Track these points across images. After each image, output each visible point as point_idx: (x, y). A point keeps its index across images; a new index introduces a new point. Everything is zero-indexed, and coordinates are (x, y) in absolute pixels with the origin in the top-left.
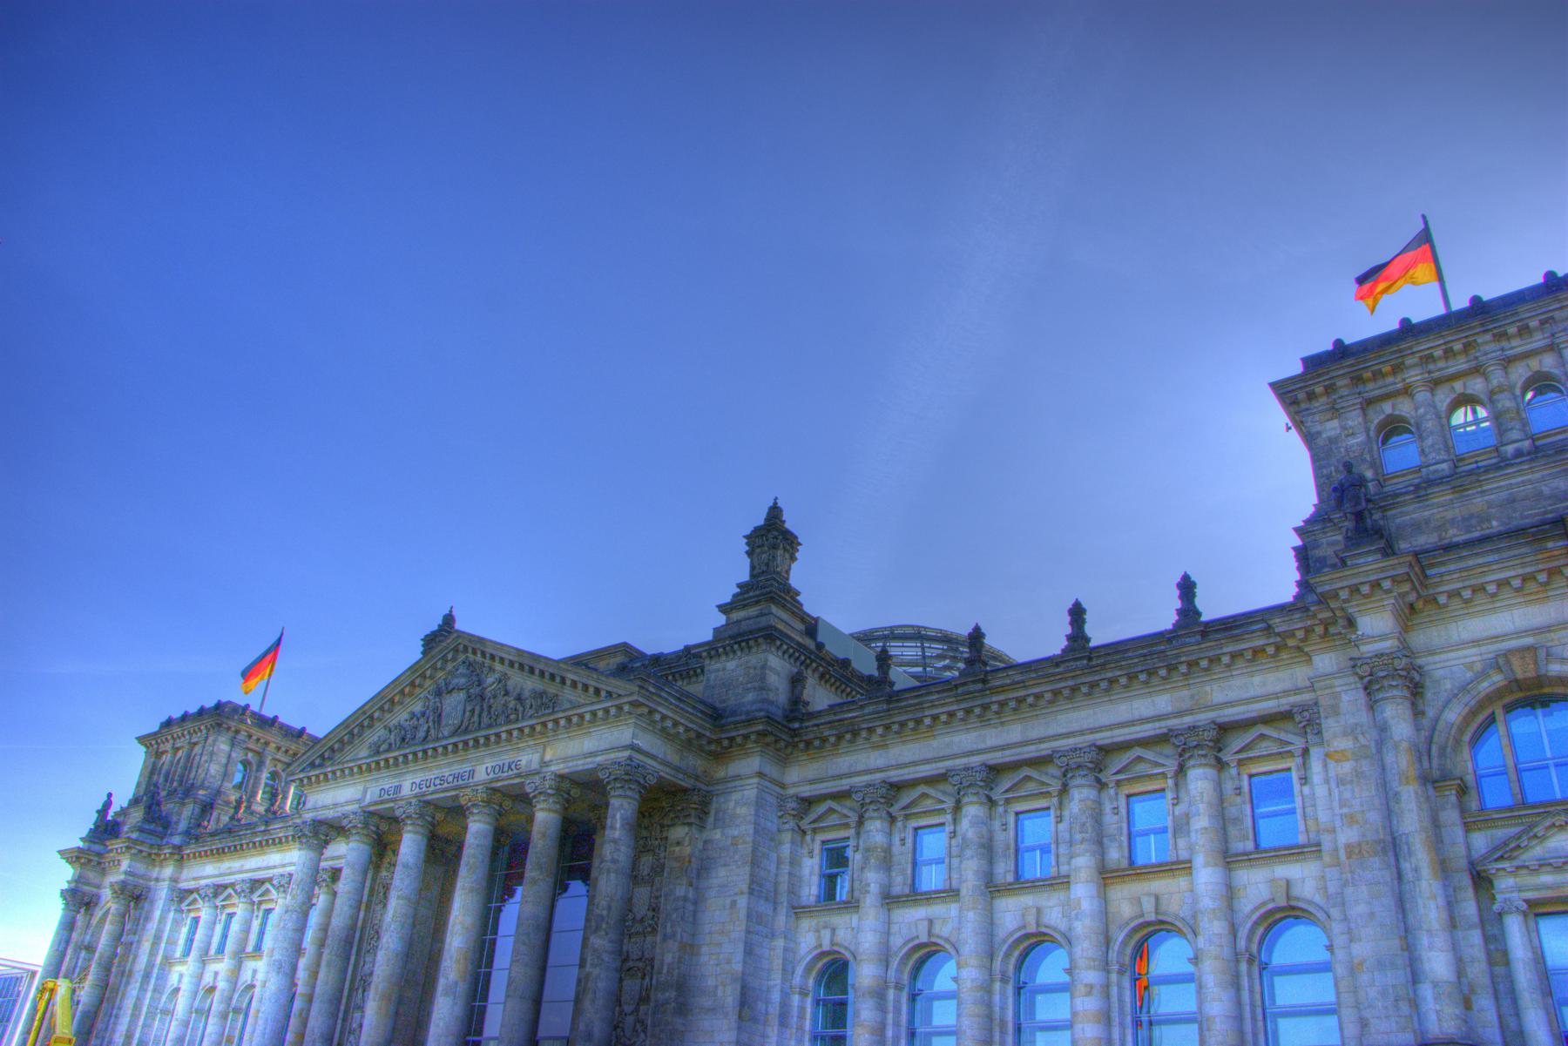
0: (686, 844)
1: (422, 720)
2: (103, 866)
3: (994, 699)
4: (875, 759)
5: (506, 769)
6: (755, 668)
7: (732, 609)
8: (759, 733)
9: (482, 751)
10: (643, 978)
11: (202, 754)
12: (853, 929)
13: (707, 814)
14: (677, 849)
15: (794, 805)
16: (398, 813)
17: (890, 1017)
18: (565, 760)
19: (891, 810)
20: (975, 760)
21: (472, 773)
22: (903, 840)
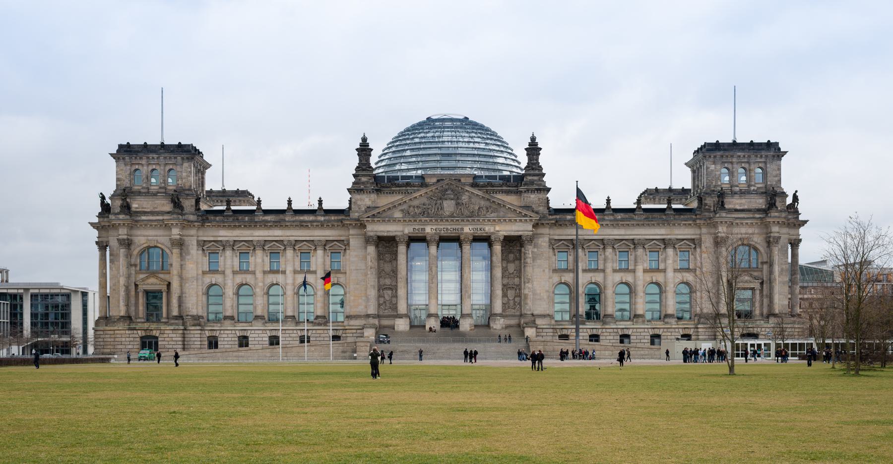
1: (430, 206)
3: (621, 223)
5: (479, 230)
8: (552, 223)
9: (467, 223)
10: (516, 290)
16: (428, 238)
18: (506, 231)
22: (585, 255)
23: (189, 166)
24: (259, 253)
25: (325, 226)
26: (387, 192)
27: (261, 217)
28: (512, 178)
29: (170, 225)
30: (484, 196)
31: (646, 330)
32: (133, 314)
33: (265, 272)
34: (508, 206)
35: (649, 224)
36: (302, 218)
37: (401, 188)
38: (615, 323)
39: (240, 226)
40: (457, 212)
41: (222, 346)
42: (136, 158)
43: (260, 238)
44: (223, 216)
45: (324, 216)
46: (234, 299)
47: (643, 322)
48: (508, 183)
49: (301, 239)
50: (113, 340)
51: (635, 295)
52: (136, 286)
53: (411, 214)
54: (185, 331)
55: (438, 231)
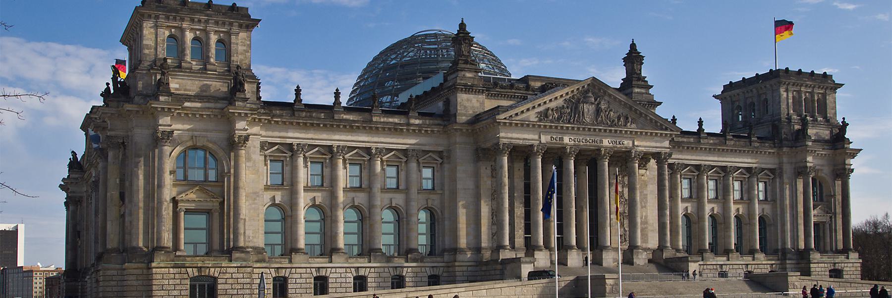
5: (618, 143)
11: (237, 44)
14: (643, 177)
18: (645, 147)
20: (707, 163)
21: (601, 142)
23: (248, 37)
26: (492, 94)
35: (740, 151)
36: (391, 120)
37: (506, 90)
39: (318, 125)
41: (294, 291)
42: (175, 19)
43: (342, 143)
45: (419, 119)
50: (140, 282)
51: (728, 228)
52: (174, 201)
55: (577, 142)
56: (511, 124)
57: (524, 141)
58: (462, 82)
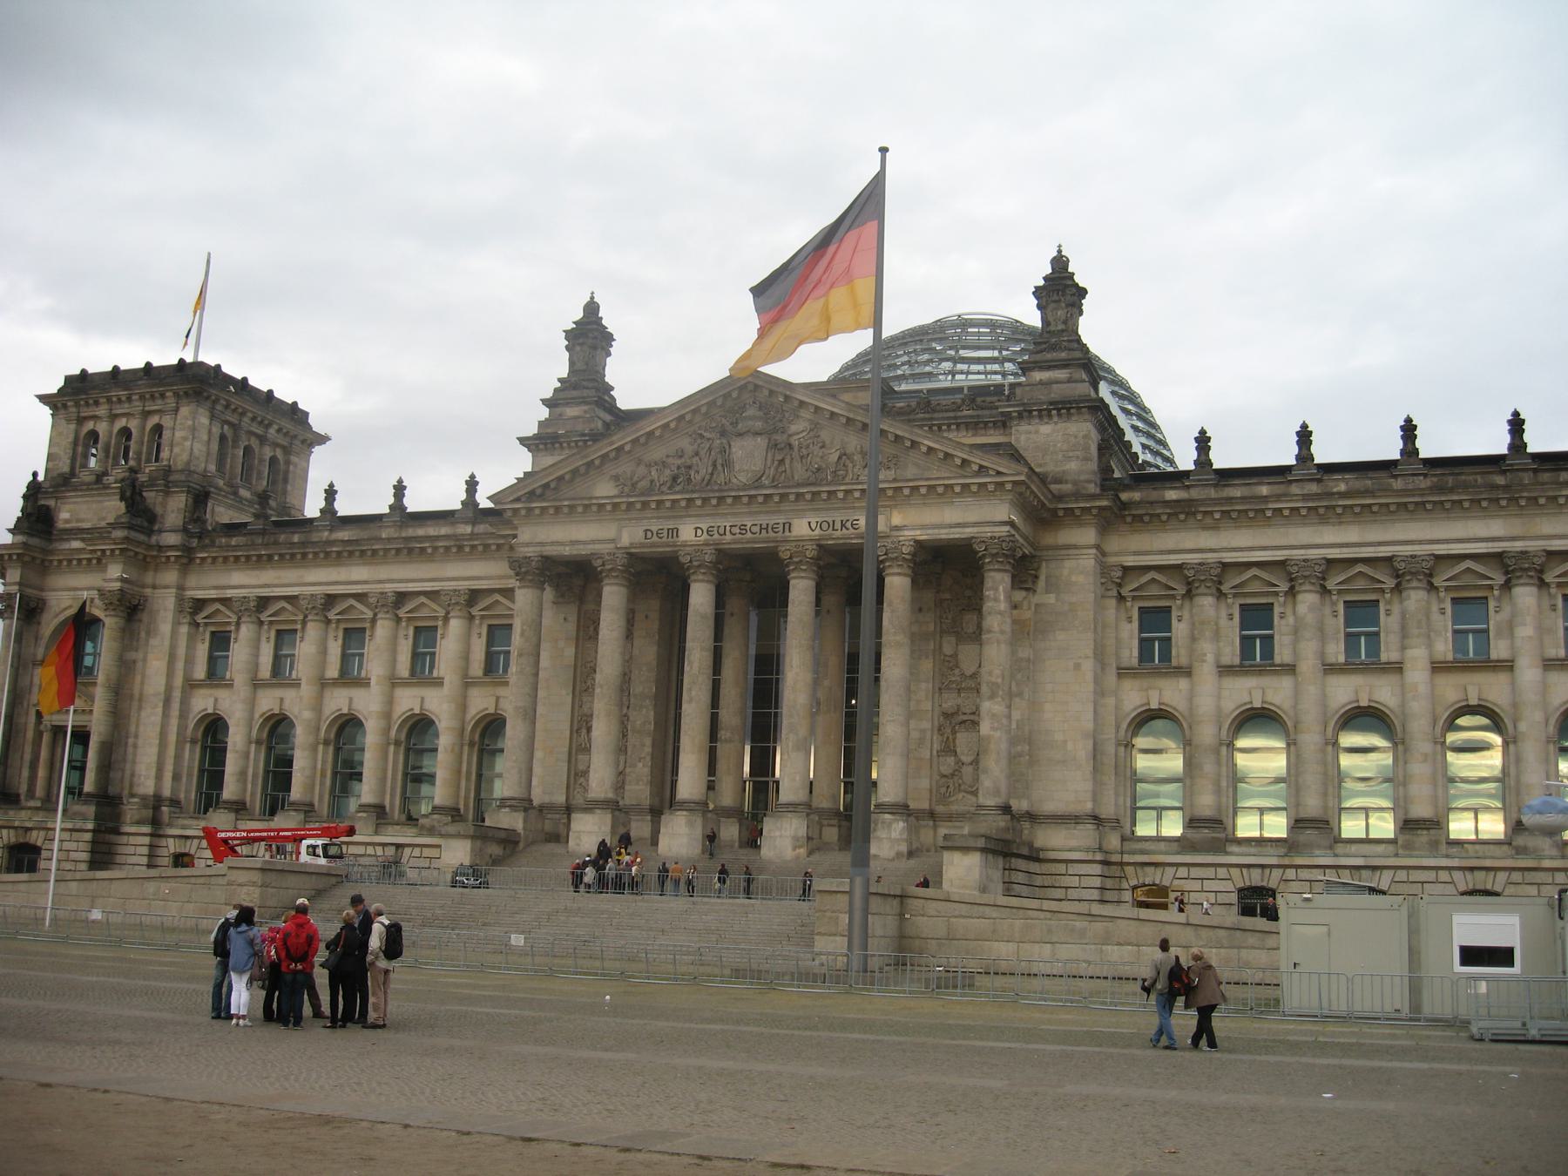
0: (1025, 608)
2: (47, 564)
3: (1340, 503)
4: (1206, 539)
5: (838, 525)
6: (1076, 437)
7: (1034, 368)
8: (1101, 508)
12: (1180, 691)
13: (1036, 577)
15: (1119, 574)
16: (685, 560)
17: (1224, 769)
18: (923, 527)
19: (1222, 588)
21: (788, 526)
22: (1230, 616)
24: (313, 630)
25: (467, 549)
27: (326, 534)
28: (1006, 393)
29: (99, 553)
30: (851, 416)
31: (1444, 875)
32: (23, 788)
33: (323, 684)
34: (926, 442)
35: (1442, 502)
36: (421, 532)
38: (1331, 848)
40: (772, 469)
42: (87, 404)
44: (245, 535)
45: (474, 524)
46: (252, 756)
47: (1434, 845)
48: (979, 400)
49: (411, 587)
51: (1406, 751)
52: (39, 715)
53: (640, 485)
54: (114, 838)
55: (716, 536)
56: (530, 510)
57: (576, 547)
58: (549, 431)
